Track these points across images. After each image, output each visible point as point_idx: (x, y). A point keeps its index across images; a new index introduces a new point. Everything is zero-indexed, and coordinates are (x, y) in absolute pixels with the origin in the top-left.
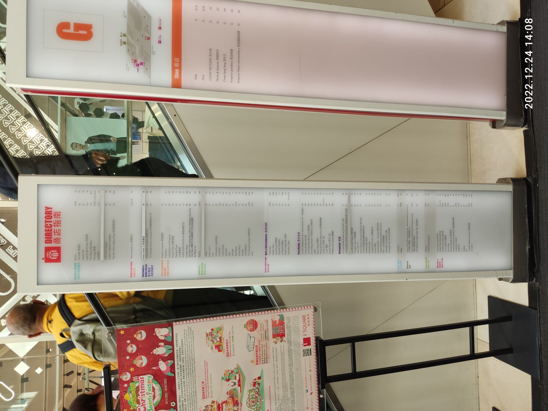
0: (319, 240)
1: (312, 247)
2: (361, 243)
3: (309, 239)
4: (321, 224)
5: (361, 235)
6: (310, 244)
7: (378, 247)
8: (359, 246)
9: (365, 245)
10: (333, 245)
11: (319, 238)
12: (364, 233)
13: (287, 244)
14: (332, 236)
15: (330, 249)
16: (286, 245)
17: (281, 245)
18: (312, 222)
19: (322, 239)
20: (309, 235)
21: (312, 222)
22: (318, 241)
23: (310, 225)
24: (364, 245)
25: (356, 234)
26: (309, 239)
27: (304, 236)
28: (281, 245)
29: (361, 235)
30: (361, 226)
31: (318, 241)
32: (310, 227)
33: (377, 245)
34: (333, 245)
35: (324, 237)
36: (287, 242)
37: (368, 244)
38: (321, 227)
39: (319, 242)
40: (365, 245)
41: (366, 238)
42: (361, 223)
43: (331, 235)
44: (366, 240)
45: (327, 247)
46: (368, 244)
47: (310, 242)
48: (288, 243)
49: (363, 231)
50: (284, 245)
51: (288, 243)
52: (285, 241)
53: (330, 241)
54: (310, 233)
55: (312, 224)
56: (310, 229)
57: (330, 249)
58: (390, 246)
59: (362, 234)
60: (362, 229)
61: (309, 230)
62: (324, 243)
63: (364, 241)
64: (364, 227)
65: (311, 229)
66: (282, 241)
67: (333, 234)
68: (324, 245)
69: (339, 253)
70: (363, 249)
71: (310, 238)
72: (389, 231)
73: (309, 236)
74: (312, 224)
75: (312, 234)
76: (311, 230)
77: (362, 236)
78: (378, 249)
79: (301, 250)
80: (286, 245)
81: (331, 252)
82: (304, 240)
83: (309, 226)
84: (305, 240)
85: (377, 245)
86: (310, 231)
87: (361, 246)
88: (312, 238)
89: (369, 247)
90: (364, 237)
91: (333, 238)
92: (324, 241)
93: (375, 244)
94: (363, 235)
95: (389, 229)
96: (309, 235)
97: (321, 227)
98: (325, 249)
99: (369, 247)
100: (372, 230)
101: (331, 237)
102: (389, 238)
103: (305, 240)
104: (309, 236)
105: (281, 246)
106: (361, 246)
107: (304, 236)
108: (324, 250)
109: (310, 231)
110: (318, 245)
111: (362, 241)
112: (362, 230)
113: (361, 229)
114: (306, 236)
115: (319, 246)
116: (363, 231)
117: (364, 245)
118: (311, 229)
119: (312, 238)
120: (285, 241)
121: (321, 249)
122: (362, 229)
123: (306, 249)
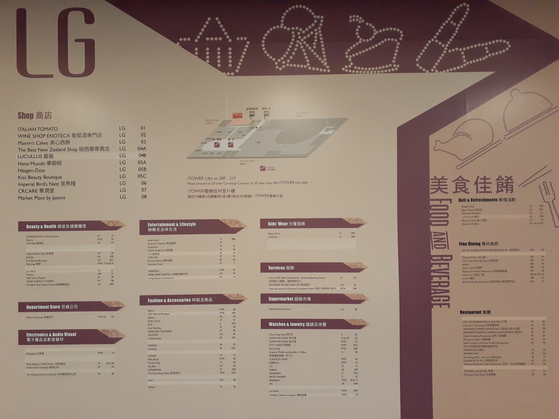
9: (475, 348)
12: (489, 346)
13: (474, 222)
24: (475, 346)
30: (498, 343)
36: (477, 222)
40: (475, 348)
42: (501, 343)
44: (480, 350)
49: (492, 346)
51: (476, 224)
52: (478, 220)
63: (479, 346)
64: (497, 346)
77: (486, 345)
90: (484, 346)
94: (487, 346)
112: (493, 345)
113: (494, 343)
116: (492, 346)
117: (475, 346)
120: (478, 220)
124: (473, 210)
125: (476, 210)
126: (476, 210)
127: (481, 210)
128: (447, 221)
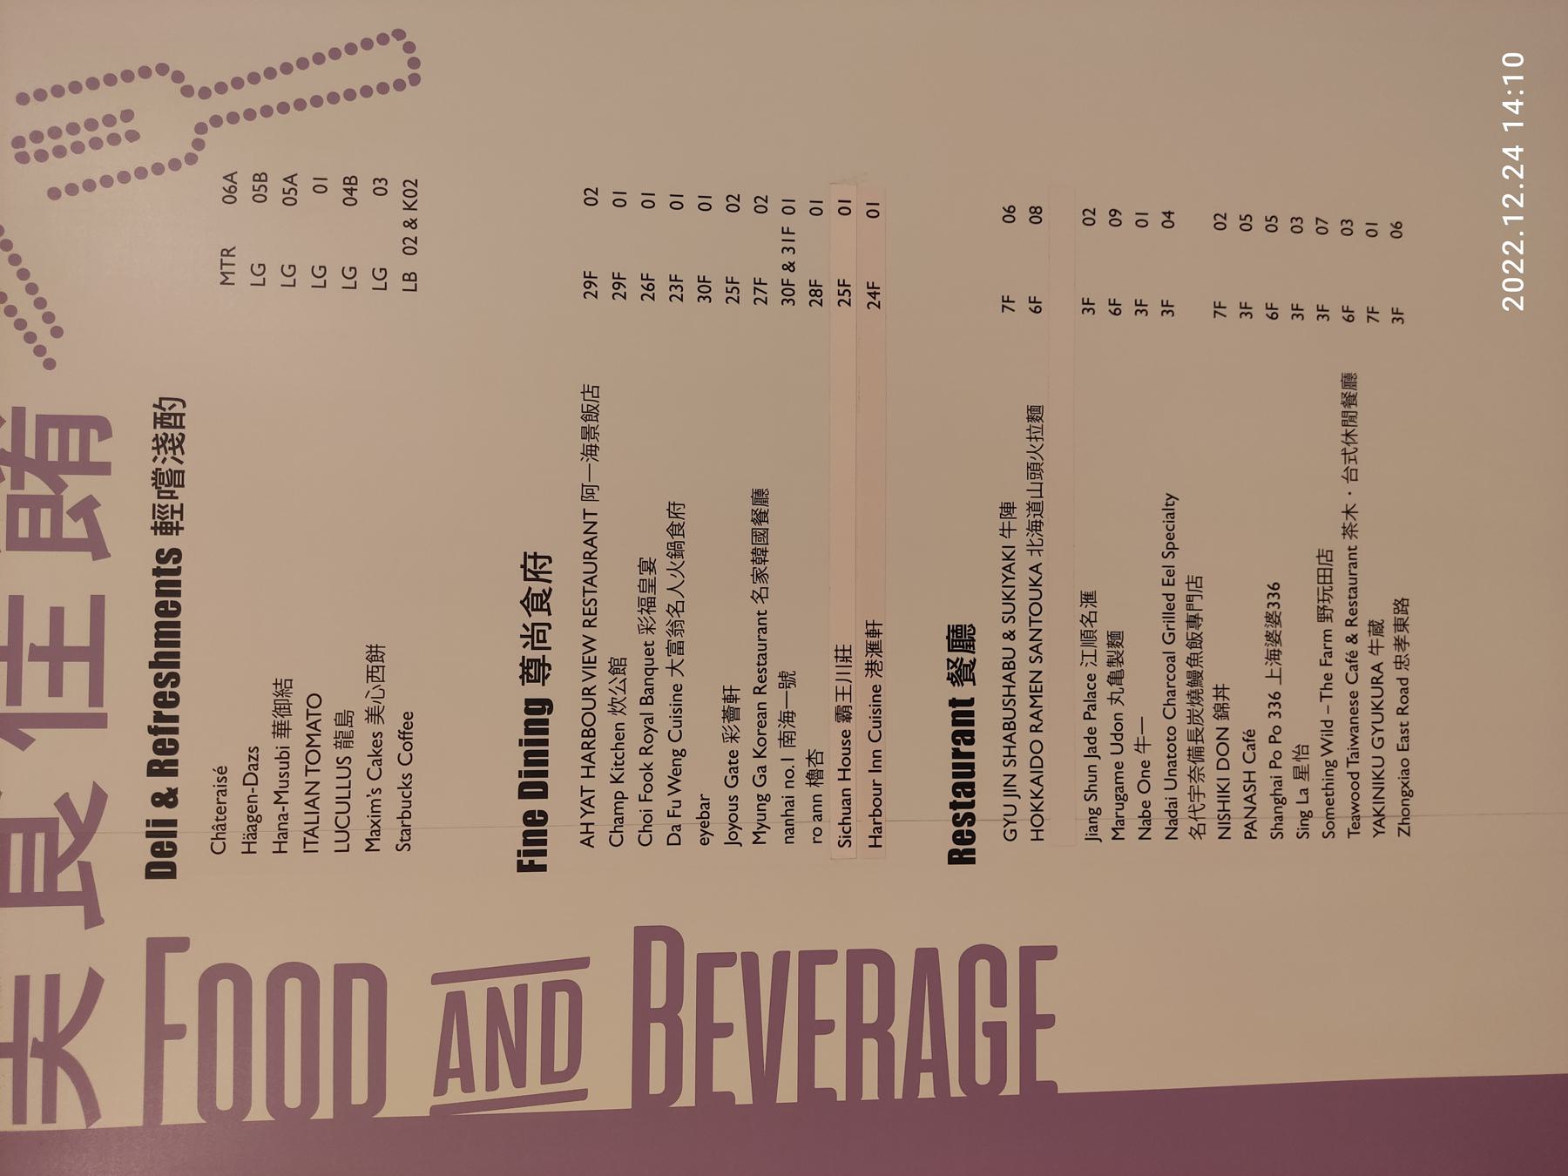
0: (747, 705)
1: (676, 774)
2: (1171, 741)
3: (647, 700)
4: (759, 556)
5: (1171, 658)
6: (660, 741)
7: (1329, 778)
8: (1159, 771)
10: (876, 754)
11: (745, 681)
14: (872, 668)
15: (847, 801)
16: (377, 758)
17: (329, 752)
18: (675, 529)
19: (774, 700)
20: (649, 653)
21: (675, 529)
22: (731, 714)
23: (663, 563)
25: (1129, 649)
26: (647, 700)
27: (602, 669)
28: (329, 752)
29: (1171, 658)
31: (731, 714)
32: (663, 578)
33: (1316, 764)
34: (876, 754)
35: (787, 680)
37: (1237, 745)
38: (760, 576)
39: (747, 724)
41: (1220, 691)
43: (860, 658)
45: (814, 777)
46: (1237, 745)
47: (663, 722)
48: (403, 735)
50: (360, 751)
53: (843, 714)
54: (660, 638)
55: (676, 550)
56: (664, 598)
57: (847, 801)
58: (1406, 771)
59: (1182, 651)
60: (1180, 603)
61: (648, 605)
62: (786, 740)
65: (675, 597)
66: (344, 718)
67: (874, 648)
68: (787, 752)
69: (956, 858)
70: (1195, 794)
71: (663, 683)
72: (1401, 625)
73: (650, 670)
74: (676, 550)
75: (676, 648)
76: (674, 609)
78: (1330, 803)
79: (560, 806)
80: (377, 758)
81: (861, 828)
82: (602, 710)
83: (647, 566)
84: (615, 707)
85: (1316, 764)
86: (661, 617)
87: (1173, 763)
88: (678, 689)
89: (1250, 783)
91: (877, 690)
92: (787, 717)
93: (1301, 751)
95: (1401, 605)
96: (649, 653)
97: (760, 576)
98: (803, 793)
99: (1250, 783)
100: (1274, 619)
101: (862, 685)
102: (1405, 690)
103: (615, 707)
104: (650, 670)
105: (328, 775)
106: (1173, 763)
107: (602, 669)
108: (790, 802)
109: (661, 617)
110: (734, 755)
111: (1182, 724)
114: (617, 667)
115: (748, 766)
118: (675, 597)
119: (678, 689)
121: (763, 799)
122: (1180, 603)
123: (620, 797)
124: (284, 756)
125: (281, 730)
126: (281, 730)
127: (283, 688)
128: (345, 974)
